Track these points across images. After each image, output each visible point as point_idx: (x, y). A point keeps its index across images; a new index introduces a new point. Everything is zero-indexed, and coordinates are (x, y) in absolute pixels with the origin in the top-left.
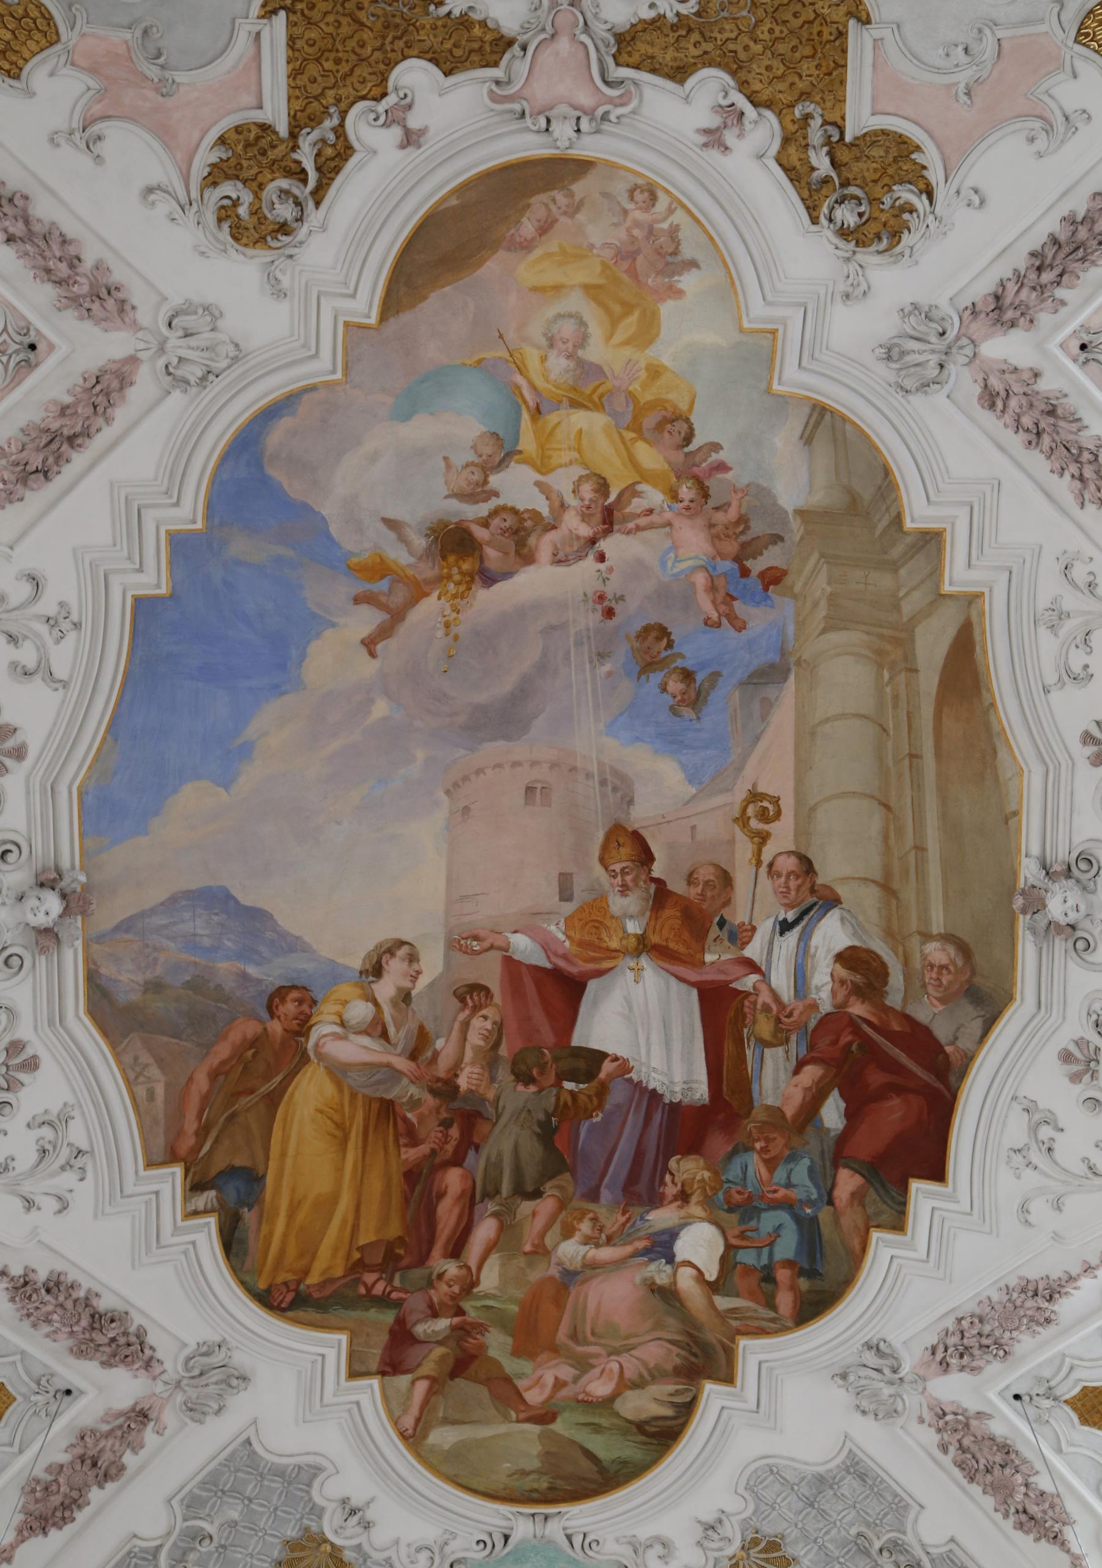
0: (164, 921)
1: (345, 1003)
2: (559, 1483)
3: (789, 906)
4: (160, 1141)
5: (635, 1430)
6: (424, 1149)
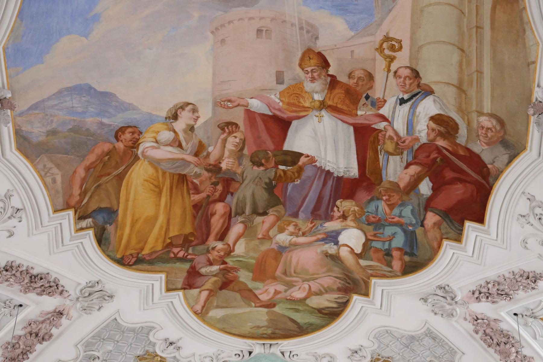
0: (56, 102)
1: (157, 132)
2: (277, 331)
3: (406, 92)
4: (60, 200)
5: (317, 312)
6: (203, 195)
